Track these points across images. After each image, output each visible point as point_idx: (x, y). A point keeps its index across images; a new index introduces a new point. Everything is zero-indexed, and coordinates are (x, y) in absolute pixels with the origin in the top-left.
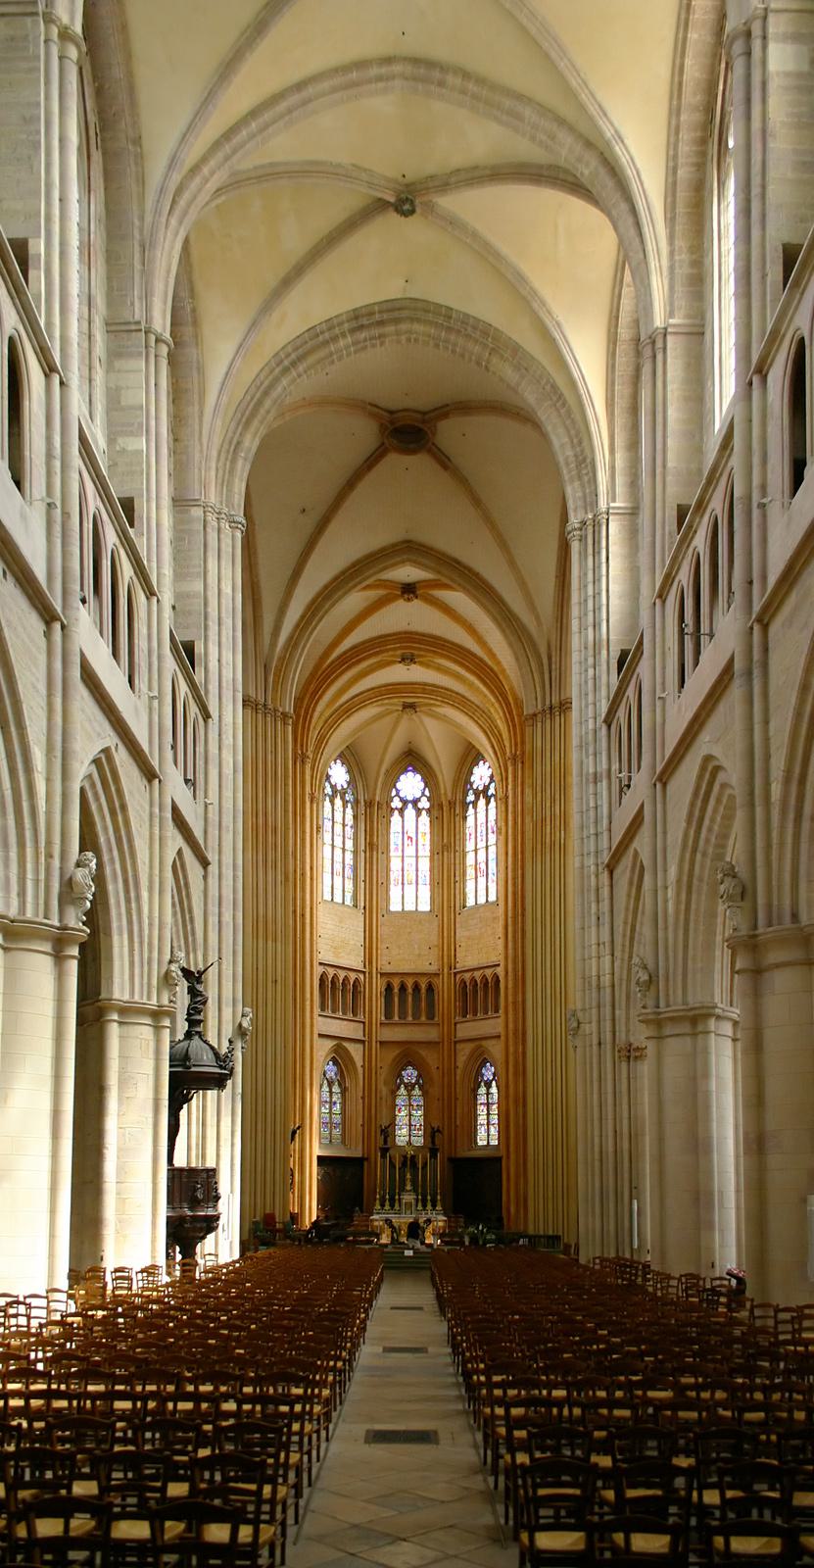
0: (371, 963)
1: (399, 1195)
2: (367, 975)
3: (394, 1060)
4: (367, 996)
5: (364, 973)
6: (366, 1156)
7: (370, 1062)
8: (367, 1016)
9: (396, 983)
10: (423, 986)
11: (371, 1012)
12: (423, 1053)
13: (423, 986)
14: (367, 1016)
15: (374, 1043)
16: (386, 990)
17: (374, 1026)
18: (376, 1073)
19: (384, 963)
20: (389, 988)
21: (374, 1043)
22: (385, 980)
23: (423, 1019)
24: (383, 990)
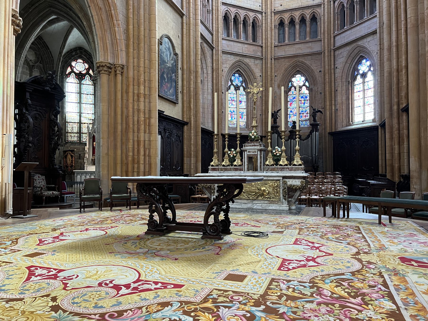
0: (266, 5)
1: (241, 147)
2: (264, 14)
3: (286, 70)
4: (264, 28)
5: (261, 13)
6: (264, 135)
7: (266, 72)
8: (264, 41)
9: (286, 17)
10: (308, 18)
11: (266, 39)
12: (308, 61)
13: (308, 18)
14: (264, 41)
15: (269, 61)
16: (279, 24)
17: (269, 48)
18: (271, 80)
19: (277, 5)
20: (281, 24)
21: (269, 61)
22: (278, 17)
23: (308, 39)
24: (277, 24)
